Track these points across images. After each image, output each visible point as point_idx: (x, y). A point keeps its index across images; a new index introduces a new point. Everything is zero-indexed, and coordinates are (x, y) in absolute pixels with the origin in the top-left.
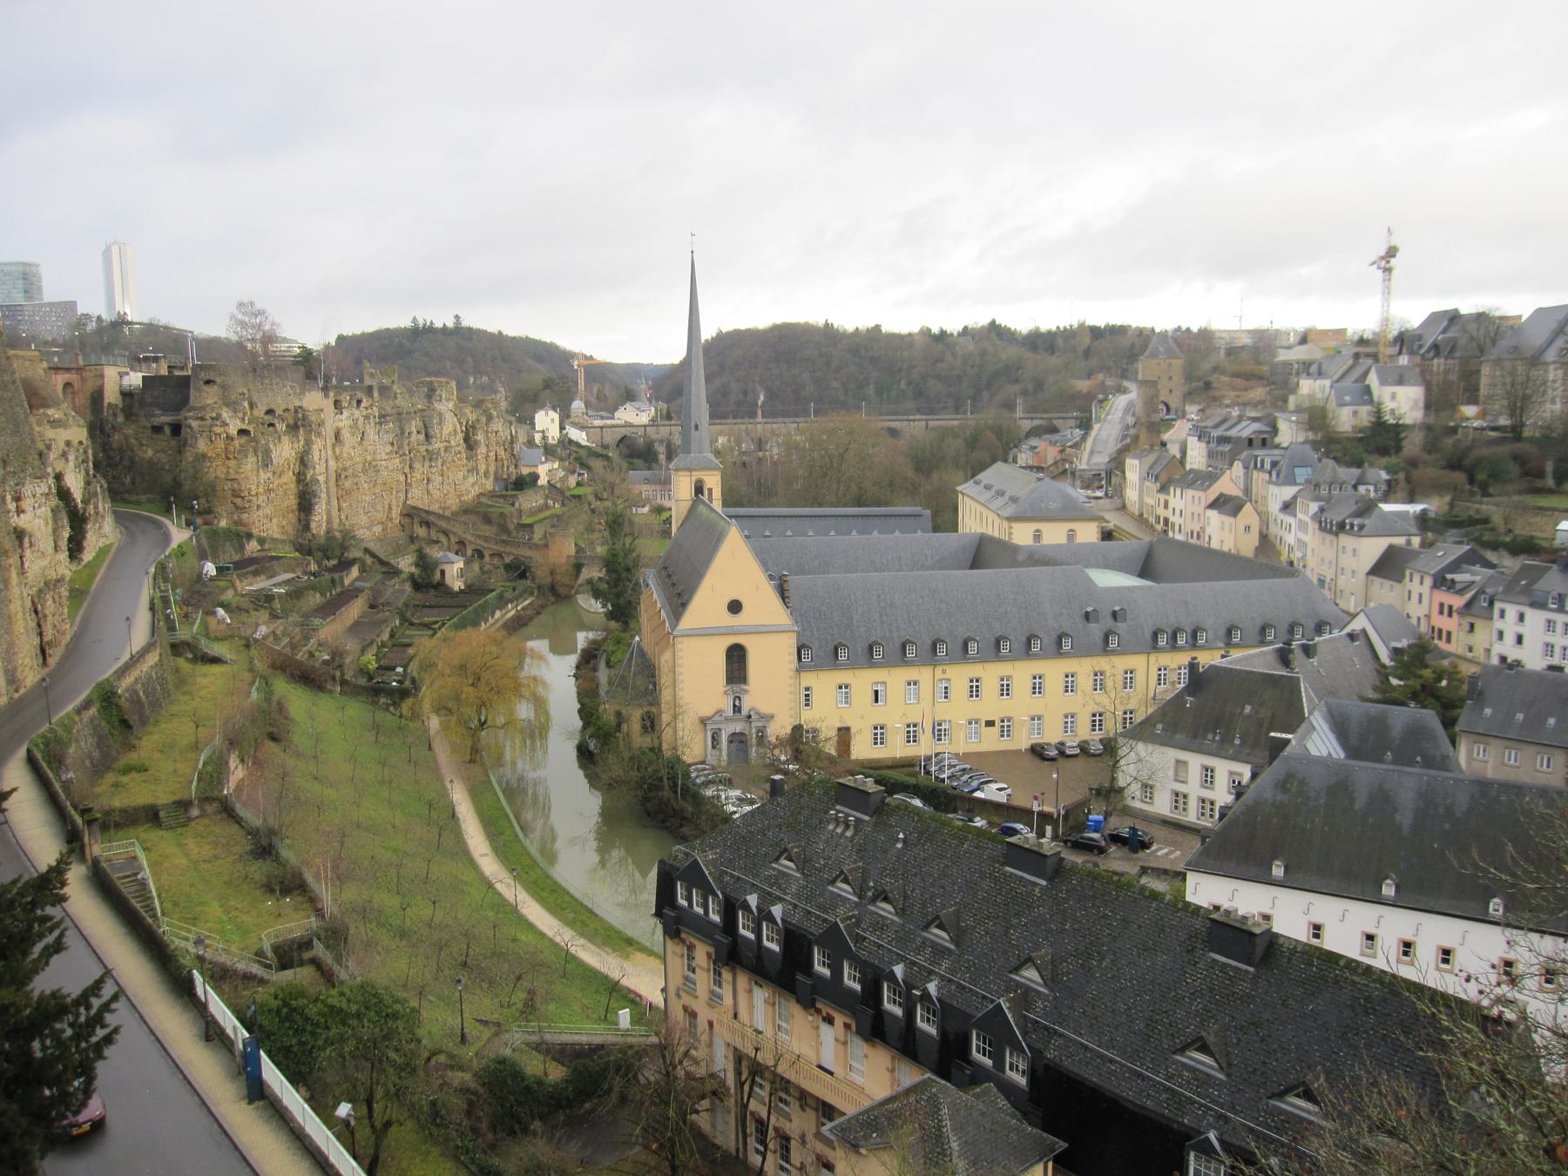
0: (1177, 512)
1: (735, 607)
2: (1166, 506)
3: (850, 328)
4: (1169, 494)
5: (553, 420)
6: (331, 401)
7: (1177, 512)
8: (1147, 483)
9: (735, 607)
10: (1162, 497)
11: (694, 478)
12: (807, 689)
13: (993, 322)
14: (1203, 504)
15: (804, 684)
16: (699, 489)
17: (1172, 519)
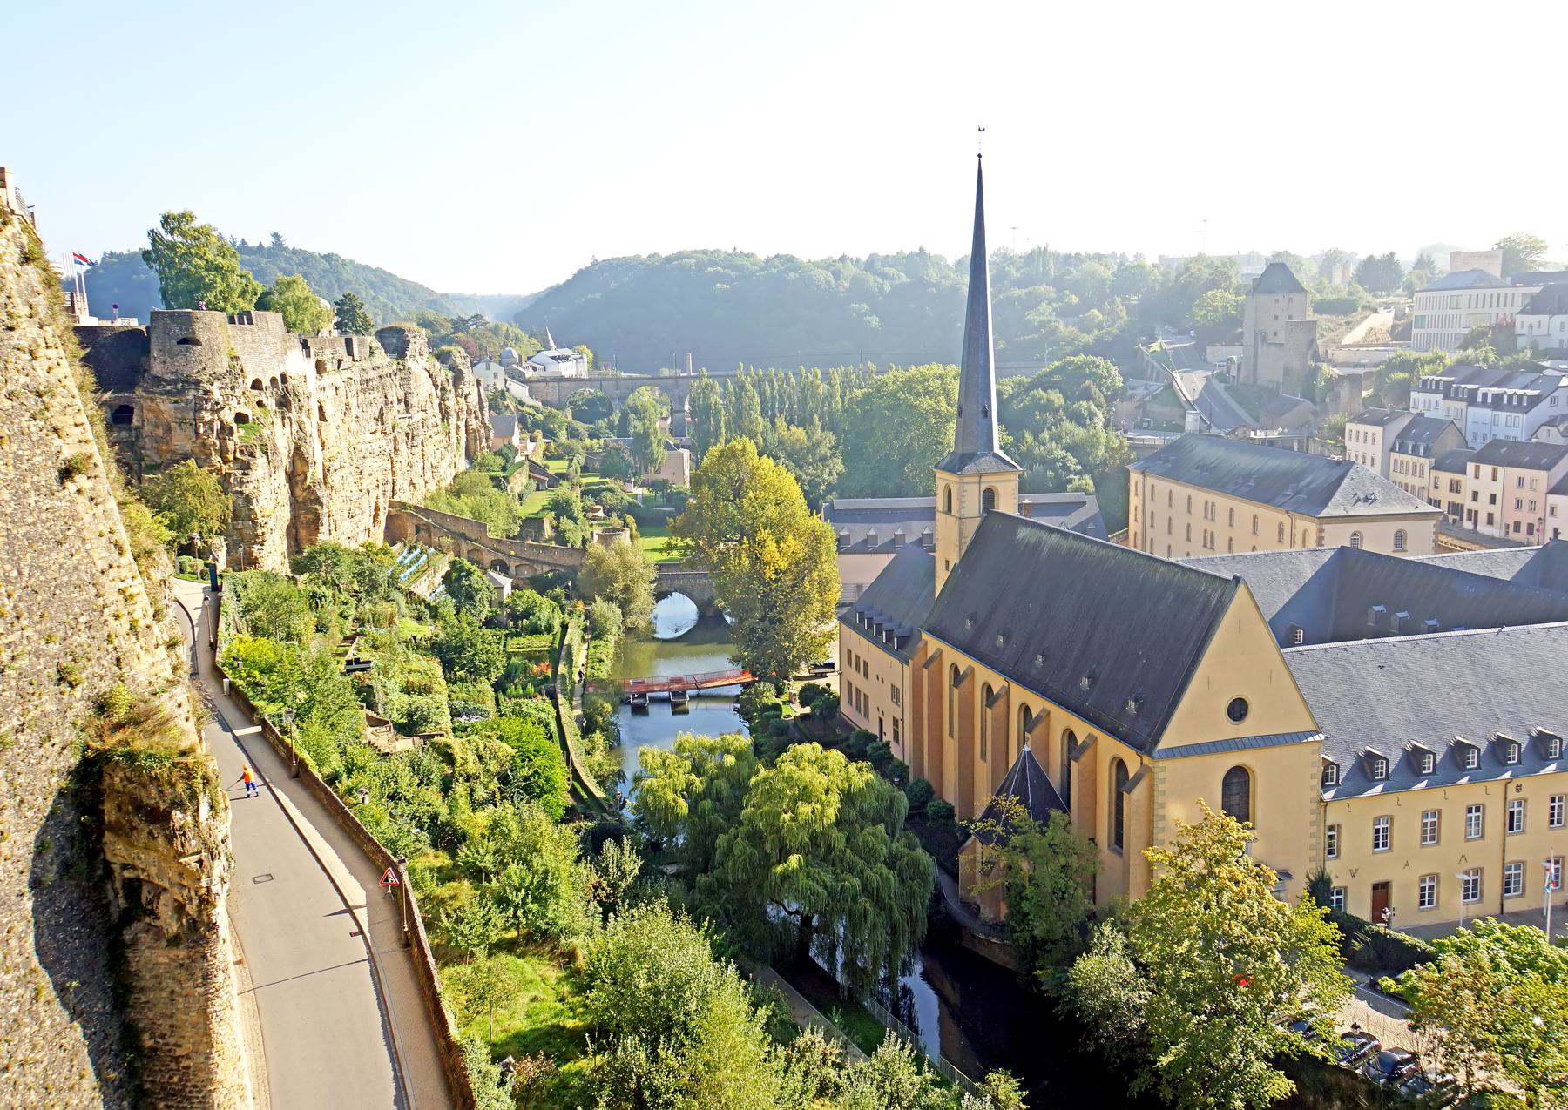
0: (1484, 498)
1: (1238, 710)
2: (1455, 487)
3: (762, 255)
4: (1464, 472)
5: (496, 376)
6: (312, 362)
7: (1484, 498)
8: (1395, 455)
9: (1238, 710)
10: (1445, 478)
11: (984, 487)
12: (1331, 828)
13: (921, 250)
14: (1544, 487)
15: (1329, 823)
16: (989, 496)
17: (1469, 505)
